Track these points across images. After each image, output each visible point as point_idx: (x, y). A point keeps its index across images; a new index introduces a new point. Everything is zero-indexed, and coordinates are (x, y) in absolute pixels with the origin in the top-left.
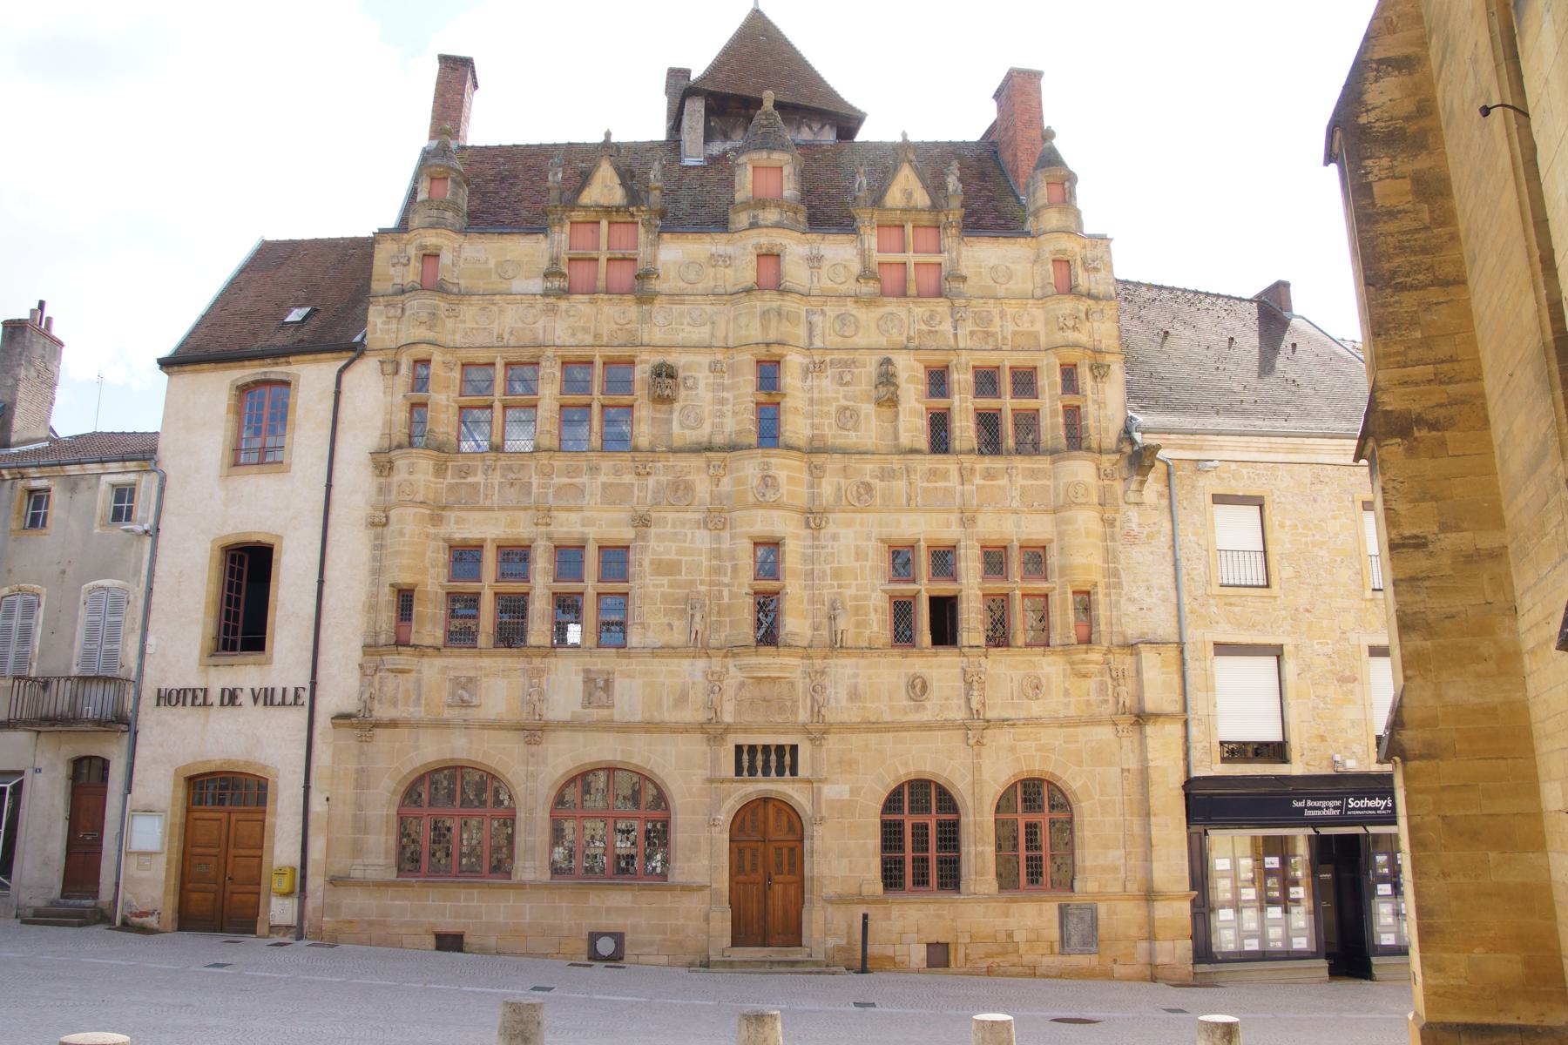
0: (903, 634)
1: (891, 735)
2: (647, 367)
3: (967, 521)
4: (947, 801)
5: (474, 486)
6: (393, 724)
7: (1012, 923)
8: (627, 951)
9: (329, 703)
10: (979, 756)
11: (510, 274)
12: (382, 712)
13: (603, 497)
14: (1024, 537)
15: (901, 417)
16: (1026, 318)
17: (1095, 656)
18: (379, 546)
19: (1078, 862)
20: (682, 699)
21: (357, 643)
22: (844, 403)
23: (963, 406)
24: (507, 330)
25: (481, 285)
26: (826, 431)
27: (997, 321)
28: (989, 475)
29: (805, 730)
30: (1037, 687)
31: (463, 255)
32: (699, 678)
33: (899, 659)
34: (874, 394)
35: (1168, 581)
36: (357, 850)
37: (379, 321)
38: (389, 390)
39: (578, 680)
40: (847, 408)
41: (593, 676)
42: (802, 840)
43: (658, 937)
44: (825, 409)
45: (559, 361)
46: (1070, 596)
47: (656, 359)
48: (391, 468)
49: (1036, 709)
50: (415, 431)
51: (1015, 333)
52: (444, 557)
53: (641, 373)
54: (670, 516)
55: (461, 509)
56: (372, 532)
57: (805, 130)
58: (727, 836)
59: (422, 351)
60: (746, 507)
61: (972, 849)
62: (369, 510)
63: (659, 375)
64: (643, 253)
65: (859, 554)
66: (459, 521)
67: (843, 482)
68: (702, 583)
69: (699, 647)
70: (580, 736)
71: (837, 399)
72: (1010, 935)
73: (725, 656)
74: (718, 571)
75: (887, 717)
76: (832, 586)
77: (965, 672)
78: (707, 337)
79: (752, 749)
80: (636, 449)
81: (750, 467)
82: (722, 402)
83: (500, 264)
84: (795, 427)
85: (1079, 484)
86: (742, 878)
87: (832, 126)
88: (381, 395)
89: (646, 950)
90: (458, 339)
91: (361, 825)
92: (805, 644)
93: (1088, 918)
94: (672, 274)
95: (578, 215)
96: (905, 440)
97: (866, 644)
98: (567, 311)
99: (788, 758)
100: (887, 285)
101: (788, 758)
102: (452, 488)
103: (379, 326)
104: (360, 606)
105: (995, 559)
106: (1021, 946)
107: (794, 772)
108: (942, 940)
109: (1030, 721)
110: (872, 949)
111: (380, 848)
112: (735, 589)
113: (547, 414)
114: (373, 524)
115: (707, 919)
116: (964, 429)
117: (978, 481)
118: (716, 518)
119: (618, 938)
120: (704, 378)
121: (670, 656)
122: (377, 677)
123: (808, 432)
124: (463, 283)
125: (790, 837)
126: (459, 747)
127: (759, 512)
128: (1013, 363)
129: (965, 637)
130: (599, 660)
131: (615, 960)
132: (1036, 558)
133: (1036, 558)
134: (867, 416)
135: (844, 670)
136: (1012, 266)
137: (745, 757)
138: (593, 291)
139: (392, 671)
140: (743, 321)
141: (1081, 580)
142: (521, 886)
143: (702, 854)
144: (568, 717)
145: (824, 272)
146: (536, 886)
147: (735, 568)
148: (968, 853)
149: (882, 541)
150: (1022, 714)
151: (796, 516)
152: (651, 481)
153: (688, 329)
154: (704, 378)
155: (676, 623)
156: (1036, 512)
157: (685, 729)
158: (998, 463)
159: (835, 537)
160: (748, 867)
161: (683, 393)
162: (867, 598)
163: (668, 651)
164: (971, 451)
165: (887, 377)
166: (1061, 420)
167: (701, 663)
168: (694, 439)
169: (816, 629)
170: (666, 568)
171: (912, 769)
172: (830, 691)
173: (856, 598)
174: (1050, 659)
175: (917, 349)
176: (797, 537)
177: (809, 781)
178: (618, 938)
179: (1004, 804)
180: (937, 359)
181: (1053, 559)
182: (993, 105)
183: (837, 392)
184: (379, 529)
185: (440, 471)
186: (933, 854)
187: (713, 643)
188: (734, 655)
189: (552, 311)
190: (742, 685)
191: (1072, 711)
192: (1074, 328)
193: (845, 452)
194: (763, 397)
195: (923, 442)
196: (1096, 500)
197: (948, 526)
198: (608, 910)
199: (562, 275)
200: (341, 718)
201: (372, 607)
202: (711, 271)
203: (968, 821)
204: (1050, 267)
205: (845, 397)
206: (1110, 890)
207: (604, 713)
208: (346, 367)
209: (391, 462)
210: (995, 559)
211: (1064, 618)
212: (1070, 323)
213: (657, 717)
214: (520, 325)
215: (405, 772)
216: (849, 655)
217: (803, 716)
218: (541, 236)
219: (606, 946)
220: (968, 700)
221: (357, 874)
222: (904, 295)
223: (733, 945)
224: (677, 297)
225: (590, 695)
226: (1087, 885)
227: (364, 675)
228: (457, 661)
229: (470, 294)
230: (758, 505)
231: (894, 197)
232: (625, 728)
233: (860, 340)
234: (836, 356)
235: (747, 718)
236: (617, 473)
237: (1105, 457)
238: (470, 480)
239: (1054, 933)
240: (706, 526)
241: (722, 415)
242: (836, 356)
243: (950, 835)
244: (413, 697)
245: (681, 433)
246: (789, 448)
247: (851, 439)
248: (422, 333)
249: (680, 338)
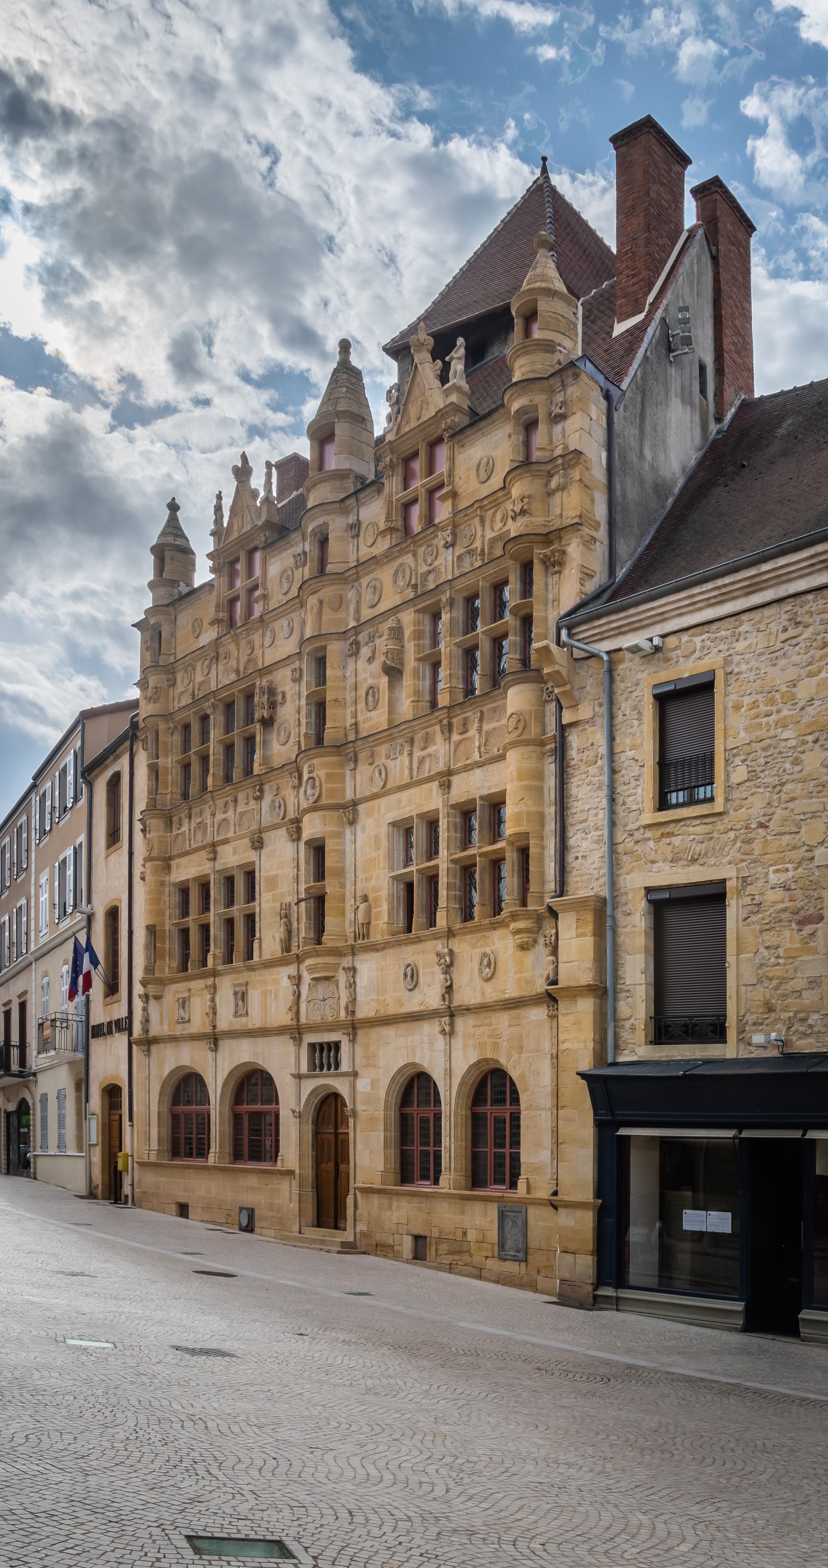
3: (446, 786)
14: (484, 792)
35: (602, 817)
72: (465, 1234)
79: (321, 1045)
93: (519, 1222)
107: (337, 1066)
108: (422, 1233)
157: (280, 1031)
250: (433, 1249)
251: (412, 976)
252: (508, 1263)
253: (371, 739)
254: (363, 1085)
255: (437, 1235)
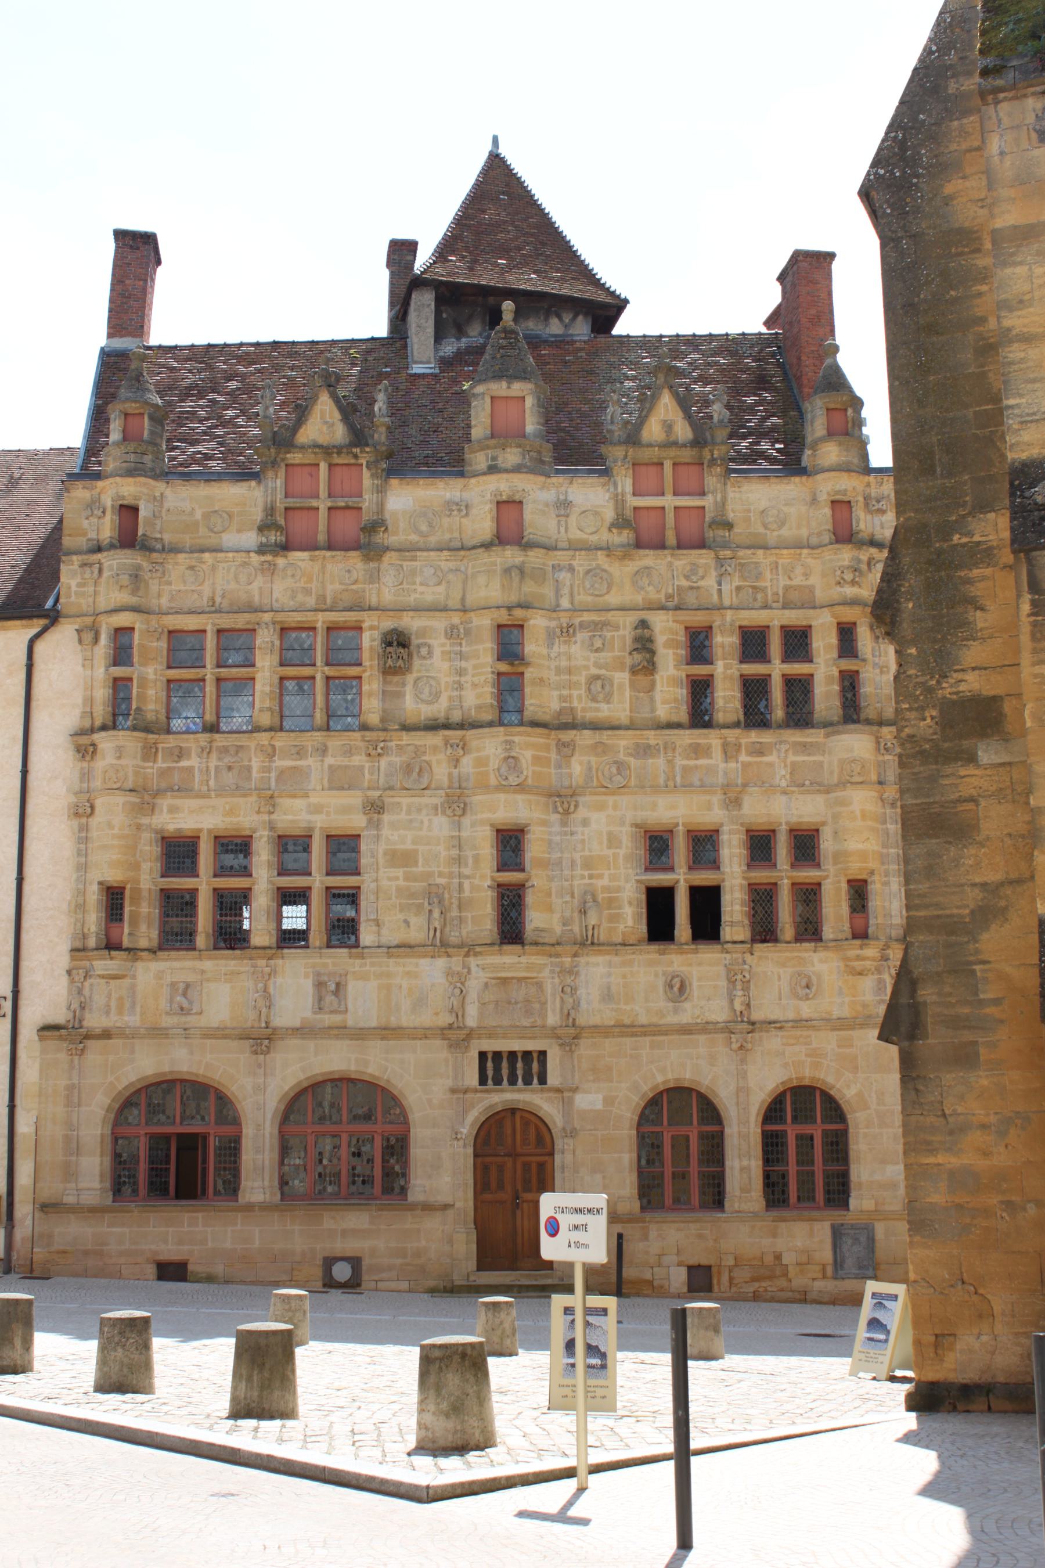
0: (659, 925)
1: (648, 1039)
2: (376, 634)
3: (734, 802)
4: (710, 1112)
5: (190, 770)
6: (106, 1035)
7: (780, 1244)
8: (365, 1277)
9: (32, 1016)
10: (743, 1061)
11: (218, 528)
12: (94, 1021)
13: (330, 781)
14: (794, 820)
15: (658, 687)
16: (799, 570)
17: (871, 951)
18: (83, 837)
19: (854, 1177)
20: (420, 1002)
21: (63, 947)
22: (594, 671)
23: (726, 672)
24: (219, 593)
25: (187, 540)
26: (575, 704)
27: (768, 575)
28: (759, 751)
29: (554, 1034)
30: (807, 986)
31: (166, 505)
32: (440, 979)
33: (656, 956)
34: (628, 661)
36: (69, 1173)
37: (73, 583)
38: (88, 662)
39: (308, 985)
40: (597, 677)
41: (325, 978)
42: (552, 1154)
43: (399, 1261)
44: (574, 678)
45: (278, 627)
46: (844, 886)
47: (388, 624)
48: (94, 752)
49: (806, 1010)
50: (119, 709)
51: (787, 588)
52: (156, 850)
53: (370, 640)
54: (405, 801)
55: (174, 797)
56: (75, 823)
57: (554, 321)
58: (470, 1151)
59: (123, 619)
60: (486, 788)
61: (737, 1164)
62: (73, 799)
63: (389, 644)
64: (368, 501)
65: (613, 841)
66: (173, 810)
67: (593, 759)
68: (441, 874)
69: (440, 945)
70: (311, 1044)
71: (587, 668)
72: (778, 1257)
73: (467, 955)
74: (459, 860)
75: (643, 1020)
76: (583, 877)
77: (729, 971)
78: (442, 598)
79: (497, 1055)
80: (364, 727)
81: (490, 745)
82: (461, 672)
83: (206, 516)
84: (541, 700)
85: (854, 761)
86: (488, 1196)
87: (586, 315)
88: (80, 668)
89: (384, 1275)
90: (164, 602)
91: (73, 1146)
92: (553, 941)
93: (863, 1239)
94: (402, 525)
95: (295, 457)
96: (663, 712)
97: (620, 940)
98: (284, 569)
99: (535, 1066)
100: (643, 535)
101: (535, 1066)
102: (163, 773)
103: (74, 588)
104: (65, 907)
105: (759, 845)
106: (790, 1268)
107: (543, 1080)
108: (704, 1262)
109: (800, 1023)
110: (628, 1272)
111: (93, 1171)
112: (476, 882)
113: (267, 689)
114: (77, 815)
115: (451, 1242)
116: (727, 699)
117: (744, 758)
118: (456, 802)
119: (355, 1262)
120: (439, 644)
121: (406, 956)
122: (87, 984)
123: (555, 705)
124: (167, 537)
125: (538, 1151)
126: (182, 1060)
127: (502, 796)
128: (785, 622)
129: (727, 932)
130: (329, 961)
131: (352, 1287)
132: (806, 844)
133: (806, 844)
134: (621, 686)
135: (596, 972)
136: (786, 509)
137: (490, 1064)
138: (311, 546)
139: (103, 977)
140: (482, 580)
141: (856, 869)
142: (249, 1207)
143: (442, 1167)
144: (297, 1023)
145: (573, 520)
146: (265, 1207)
147: (477, 859)
148: (732, 1168)
149: (637, 826)
150: (791, 1015)
151: (543, 799)
152: (383, 762)
153: (420, 589)
154: (439, 644)
155: (414, 920)
156: (808, 792)
157: (424, 1034)
158: (766, 737)
159: (585, 822)
160: (494, 1185)
161: (417, 662)
162: (618, 889)
163: (405, 948)
164: (736, 725)
165: (644, 643)
166: (836, 688)
167: (441, 963)
168: (430, 715)
169: (564, 925)
170: (402, 858)
171: (670, 1076)
172: (582, 992)
173: (606, 889)
174: (822, 954)
175: (677, 608)
176: (544, 823)
177: (558, 1090)
178: (355, 1262)
179: (773, 1112)
180: (698, 619)
181: (827, 844)
182: (778, 288)
183: (588, 659)
184: (84, 820)
185: (150, 753)
186: (694, 1168)
187: (453, 937)
188: (476, 954)
189: (270, 570)
190: (486, 984)
191: (846, 1012)
192: (853, 583)
193: (596, 726)
194: (503, 667)
195: (683, 715)
196: (874, 777)
197: (709, 808)
198: (344, 1233)
199: (278, 527)
200: (48, 1029)
201: (79, 907)
202: (446, 521)
203: (732, 1132)
204: (827, 511)
205: (597, 665)
206: (887, 1208)
207: (337, 1019)
208: (38, 636)
209: (93, 745)
210: (759, 845)
211: (834, 909)
212: (848, 577)
213: (393, 1022)
214: (233, 586)
215: (120, 1087)
216: (600, 953)
217: (552, 1019)
218: (253, 483)
219: (342, 1272)
220: (732, 1001)
221: (70, 1199)
222: (662, 546)
223: (479, 1269)
224: (407, 550)
225: (320, 999)
226: (860, 1202)
227: (72, 981)
228: (176, 964)
229: (175, 550)
230: (500, 788)
231: (653, 430)
232: (360, 1034)
233: (613, 599)
234: (587, 617)
235: (491, 1022)
236: (349, 752)
237: (885, 730)
238: (184, 763)
239: (827, 1255)
240: (444, 813)
241: (460, 687)
242: (587, 617)
243: (714, 1148)
244: (127, 1005)
245: (413, 705)
246: (535, 724)
247: (604, 711)
248: (124, 597)
249: (411, 599)
250: (725, 1278)
251: (679, 989)
252: (847, 1281)
253: (609, 732)
254: (588, 1101)
255: (732, 1262)
